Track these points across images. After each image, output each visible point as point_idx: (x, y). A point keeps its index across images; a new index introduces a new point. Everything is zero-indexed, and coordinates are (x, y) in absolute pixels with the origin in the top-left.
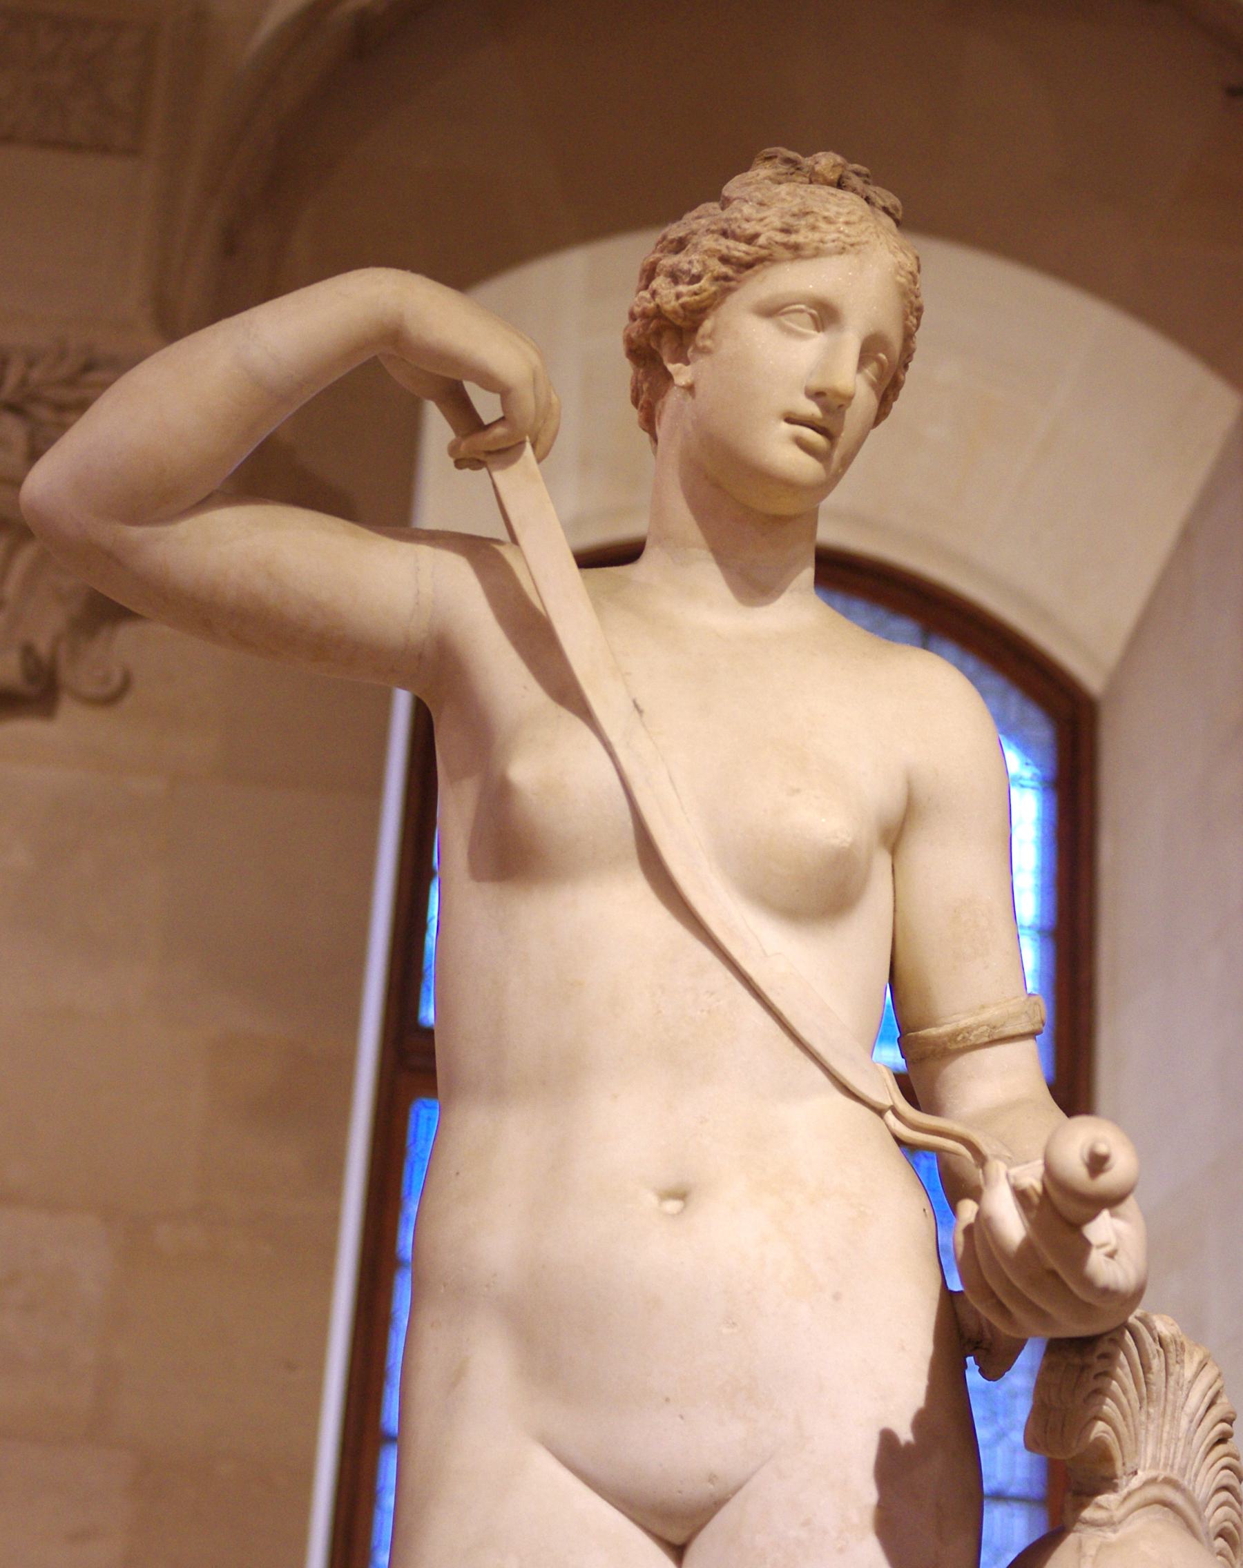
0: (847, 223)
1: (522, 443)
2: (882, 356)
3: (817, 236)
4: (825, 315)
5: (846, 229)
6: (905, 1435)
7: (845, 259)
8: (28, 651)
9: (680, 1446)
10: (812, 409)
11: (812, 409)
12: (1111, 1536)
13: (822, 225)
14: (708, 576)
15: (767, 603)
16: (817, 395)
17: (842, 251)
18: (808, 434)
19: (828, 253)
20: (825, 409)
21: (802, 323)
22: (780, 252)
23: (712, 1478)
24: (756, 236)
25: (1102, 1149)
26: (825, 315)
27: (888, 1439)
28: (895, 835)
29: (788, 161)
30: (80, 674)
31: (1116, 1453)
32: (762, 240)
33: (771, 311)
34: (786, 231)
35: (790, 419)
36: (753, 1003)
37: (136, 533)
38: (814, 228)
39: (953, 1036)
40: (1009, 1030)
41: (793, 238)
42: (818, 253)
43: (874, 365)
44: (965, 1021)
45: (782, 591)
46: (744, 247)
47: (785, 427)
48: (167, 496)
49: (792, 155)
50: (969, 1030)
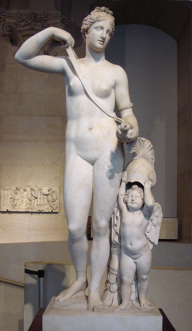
1: (69, 46)
2: (109, 32)
3: (100, 19)
4: (102, 28)
6: (114, 152)
7: (104, 21)
9: (92, 155)
10: (101, 39)
11: (101, 39)
13: (101, 17)
14: (92, 59)
15: (98, 62)
16: (101, 38)
17: (103, 20)
19: (102, 21)
20: (103, 39)
21: (99, 29)
22: (97, 21)
23: (95, 158)
24: (94, 19)
26: (102, 28)
27: (112, 153)
28: (114, 87)
32: (94, 20)
33: (96, 28)
34: (97, 18)
35: (99, 41)
36: (98, 108)
38: (100, 18)
39: (122, 108)
41: (98, 19)
42: (101, 21)
44: (123, 107)
45: (100, 60)
46: (92, 21)
47: (98, 42)
50: (123, 108)
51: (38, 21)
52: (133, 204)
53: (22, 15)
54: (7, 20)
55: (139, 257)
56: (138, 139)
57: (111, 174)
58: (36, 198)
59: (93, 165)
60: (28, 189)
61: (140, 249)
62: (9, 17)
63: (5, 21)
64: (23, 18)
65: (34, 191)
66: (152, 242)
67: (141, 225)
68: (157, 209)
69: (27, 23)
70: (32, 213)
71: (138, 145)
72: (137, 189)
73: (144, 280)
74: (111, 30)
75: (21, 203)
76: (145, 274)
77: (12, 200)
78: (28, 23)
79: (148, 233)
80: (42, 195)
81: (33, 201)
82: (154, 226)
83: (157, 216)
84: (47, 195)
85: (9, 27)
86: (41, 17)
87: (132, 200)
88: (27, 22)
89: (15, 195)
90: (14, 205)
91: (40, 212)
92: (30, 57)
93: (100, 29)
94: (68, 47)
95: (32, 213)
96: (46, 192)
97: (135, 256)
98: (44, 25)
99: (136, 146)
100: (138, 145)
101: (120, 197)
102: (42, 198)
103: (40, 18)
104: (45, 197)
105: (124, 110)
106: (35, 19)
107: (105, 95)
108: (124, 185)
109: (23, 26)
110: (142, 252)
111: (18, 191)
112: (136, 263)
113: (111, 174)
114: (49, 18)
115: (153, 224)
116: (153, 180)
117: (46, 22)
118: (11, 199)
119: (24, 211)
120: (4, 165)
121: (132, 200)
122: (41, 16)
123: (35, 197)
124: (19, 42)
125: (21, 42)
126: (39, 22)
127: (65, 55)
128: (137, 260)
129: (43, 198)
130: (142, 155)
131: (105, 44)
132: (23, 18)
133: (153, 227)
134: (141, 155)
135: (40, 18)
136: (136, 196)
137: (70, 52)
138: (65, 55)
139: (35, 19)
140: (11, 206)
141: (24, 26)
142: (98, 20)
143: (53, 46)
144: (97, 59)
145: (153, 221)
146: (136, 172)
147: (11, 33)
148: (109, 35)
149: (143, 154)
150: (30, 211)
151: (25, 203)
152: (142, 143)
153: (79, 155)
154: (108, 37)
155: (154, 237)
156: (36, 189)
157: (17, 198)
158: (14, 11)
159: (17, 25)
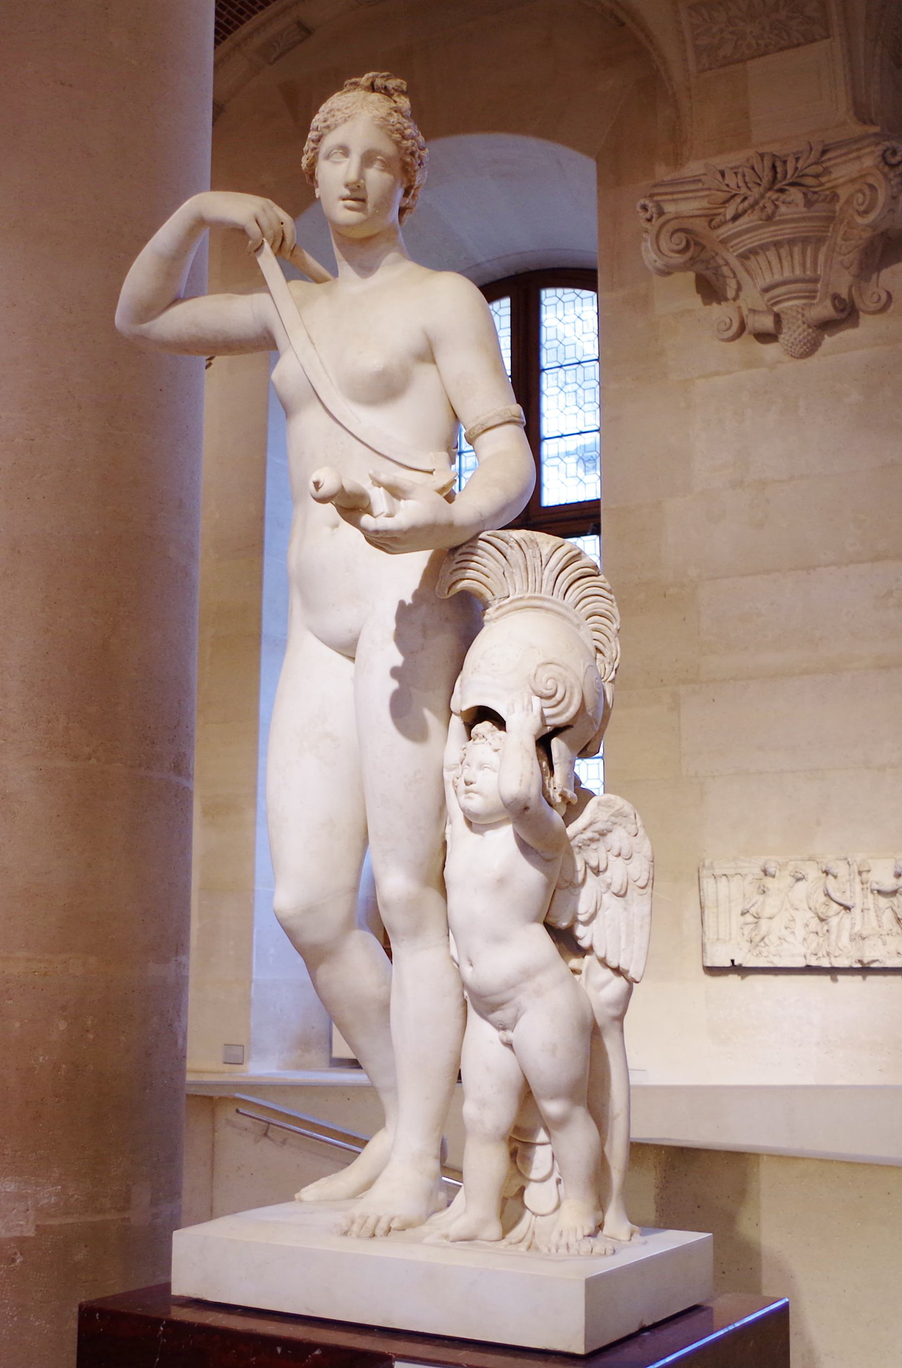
0: (346, 108)
5: (346, 111)
6: (409, 600)
7: (349, 124)
8: (836, 297)
10: (346, 192)
11: (346, 192)
12: (493, 624)
13: (337, 113)
16: (347, 186)
20: (352, 190)
21: (338, 157)
22: (326, 131)
23: (350, 631)
26: (345, 151)
27: (402, 604)
28: (428, 355)
29: (351, 84)
30: (867, 302)
31: (483, 590)
33: (328, 157)
35: (344, 199)
37: (145, 326)
38: (333, 116)
40: (490, 424)
41: (328, 123)
42: (336, 126)
43: (378, 162)
45: (378, 268)
47: (342, 202)
48: (150, 309)
49: (353, 80)
50: (474, 428)
51: (792, 184)
52: (470, 798)
53: (723, 174)
54: (670, 209)
55: (516, 1020)
56: (481, 536)
58: (847, 908)
60: (812, 872)
61: (512, 985)
62: (675, 196)
63: (661, 213)
64: (727, 185)
65: (835, 877)
66: (614, 964)
67: (502, 882)
68: (614, 824)
69: (746, 204)
70: (833, 972)
71: (491, 564)
72: (488, 736)
73: (562, 1122)
74: (388, 149)
75: (785, 933)
76: (554, 1097)
77: (749, 918)
78: (751, 200)
80: (870, 896)
81: (834, 921)
82: (617, 895)
83: (624, 852)
84: (894, 893)
85: (682, 235)
86: (800, 165)
87: (467, 783)
88: (745, 199)
89: (761, 898)
90: (758, 939)
91: (865, 970)
92: (150, 309)
93: (339, 154)
94: (259, 248)
95: (833, 972)
97: (497, 1015)
98: (815, 193)
99: (473, 564)
101: (446, 775)
102: (871, 906)
103: (796, 169)
104: (883, 902)
105: (479, 435)
106: (775, 178)
107: (386, 389)
109: (735, 218)
110: (522, 999)
111: (768, 881)
112: (509, 1045)
114: (829, 159)
115: (609, 886)
116: (558, 696)
117: (823, 180)
118: (743, 914)
119: (801, 963)
120: (714, 777)
121: (467, 783)
122: (797, 159)
123: (841, 905)
124: (732, 284)
125: (738, 283)
126: (792, 190)
128: (510, 1035)
129: (877, 909)
130: (521, 599)
131: (369, 207)
132: (727, 185)
133: (608, 899)
134: (511, 602)
135: (796, 169)
137: (268, 262)
139: (775, 178)
140: (746, 946)
141: (735, 218)
142: (328, 127)
144: (366, 269)
145: (608, 874)
146: (479, 666)
147: (689, 255)
148: (382, 170)
149: (528, 594)
150: (825, 963)
151: (800, 932)
152: (514, 554)
153: (310, 629)
154: (376, 178)
155: (623, 946)
156: (841, 869)
157: (767, 912)
158: (693, 168)
159: (710, 218)
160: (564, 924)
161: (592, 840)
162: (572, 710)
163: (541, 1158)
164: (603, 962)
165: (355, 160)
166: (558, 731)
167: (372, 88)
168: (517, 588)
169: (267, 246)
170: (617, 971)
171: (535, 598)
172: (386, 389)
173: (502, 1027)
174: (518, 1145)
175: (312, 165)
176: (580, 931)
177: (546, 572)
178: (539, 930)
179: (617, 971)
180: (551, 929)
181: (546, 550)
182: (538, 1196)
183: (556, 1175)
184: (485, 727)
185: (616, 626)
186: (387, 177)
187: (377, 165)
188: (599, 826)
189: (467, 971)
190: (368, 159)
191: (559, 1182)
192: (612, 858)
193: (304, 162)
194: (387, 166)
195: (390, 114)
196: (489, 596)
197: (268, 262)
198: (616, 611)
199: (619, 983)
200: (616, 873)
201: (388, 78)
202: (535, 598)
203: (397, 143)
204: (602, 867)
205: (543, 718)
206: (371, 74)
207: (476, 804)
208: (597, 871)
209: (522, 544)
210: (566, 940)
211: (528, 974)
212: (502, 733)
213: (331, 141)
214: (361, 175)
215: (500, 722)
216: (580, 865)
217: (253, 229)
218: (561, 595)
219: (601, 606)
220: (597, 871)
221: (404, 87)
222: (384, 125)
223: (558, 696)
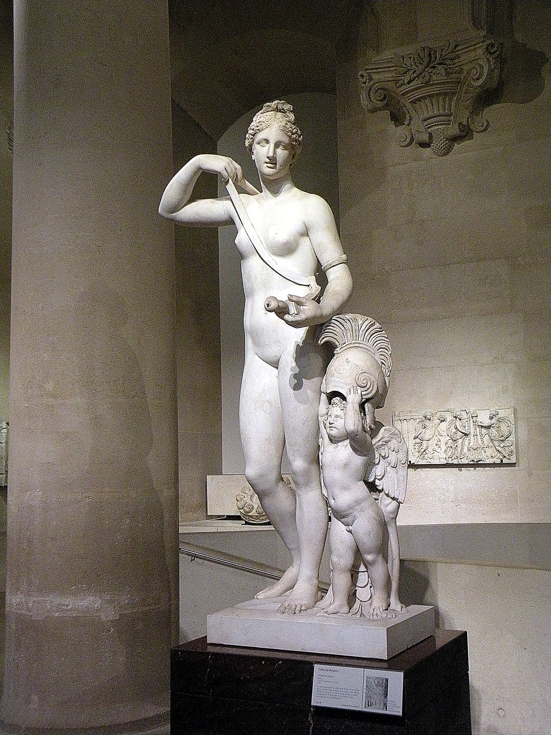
6: (301, 345)
13: (263, 123)
17: (267, 128)
18: (269, 165)
25: (267, 303)
26: (267, 141)
27: (298, 345)
28: (306, 233)
31: (335, 341)
41: (259, 128)
42: (263, 130)
47: (266, 165)
51: (438, 64)
53: (403, 57)
54: (376, 77)
57: (296, 381)
58: (466, 435)
59: (277, 368)
60: (449, 418)
61: (350, 507)
62: (378, 70)
63: (371, 79)
64: (405, 64)
65: (460, 420)
66: (392, 496)
67: (346, 465)
69: (415, 75)
70: (460, 466)
71: (338, 330)
73: (373, 563)
74: (286, 140)
75: (436, 447)
76: (369, 553)
77: (418, 441)
78: (418, 72)
79: (379, 480)
80: (478, 429)
81: (460, 441)
85: (382, 91)
88: (415, 72)
89: (424, 430)
90: (423, 450)
91: (476, 465)
92: (176, 208)
95: (460, 466)
96: (487, 422)
98: (450, 68)
100: (338, 330)
102: (478, 434)
103: (442, 55)
104: (484, 431)
106: (430, 60)
107: (287, 250)
108: (324, 397)
109: (409, 83)
110: (356, 513)
111: (427, 423)
112: (350, 531)
113: (296, 381)
114: (459, 50)
116: (368, 387)
117: (456, 61)
118: (415, 438)
119: (444, 462)
122: (442, 50)
123: (463, 433)
124: (408, 117)
125: (410, 116)
126: (440, 67)
127: (226, 195)
128: (351, 528)
129: (481, 434)
132: (405, 64)
135: (442, 55)
136: (337, 416)
137: (231, 188)
138: (226, 195)
139: (430, 60)
140: (417, 454)
141: (409, 83)
142: (258, 130)
143: (208, 185)
144: (275, 192)
147: (385, 102)
149: (353, 342)
150: (455, 462)
151: (444, 447)
152: (348, 325)
154: (281, 153)
155: (396, 488)
156: (464, 415)
157: (427, 437)
158: (388, 54)
159: (397, 82)
160: (371, 480)
161: (382, 445)
162: (374, 392)
163: (363, 578)
164: (388, 495)
165: (272, 145)
166: (367, 400)
167: (277, 110)
168: (349, 339)
169: (230, 180)
170: (393, 499)
171: (356, 343)
172: (287, 250)
173: (347, 525)
174: (354, 573)
175: (251, 145)
176: (377, 482)
177: (361, 332)
178: (362, 483)
179: (393, 499)
180: (366, 482)
181: (360, 322)
182: (362, 594)
183: (369, 585)
184: (336, 400)
185: (390, 352)
186: (286, 152)
187: (281, 147)
188: (385, 439)
189: (332, 502)
190: (277, 145)
191: (371, 587)
192: (390, 452)
193: (247, 144)
194: (285, 148)
195: (286, 124)
196: (337, 343)
197: (231, 188)
198: (389, 346)
199: (394, 503)
200: (393, 458)
201: (284, 104)
202: (356, 343)
203: (290, 137)
204: (387, 456)
205: (362, 396)
206: (276, 102)
207: (334, 432)
208: (384, 458)
209: (350, 320)
210: (372, 487)
211: (358, 502)
212: (344, 402)
213: (260, 136)
214: (275, 153)
215: (344, 398)
216: (377, 456)
217: (225, 173)
218: (367, 341)
219: (384, 345)
220: (384, 458)
221: (292, 109)
222: (284, 130)
223: (368, 387)
